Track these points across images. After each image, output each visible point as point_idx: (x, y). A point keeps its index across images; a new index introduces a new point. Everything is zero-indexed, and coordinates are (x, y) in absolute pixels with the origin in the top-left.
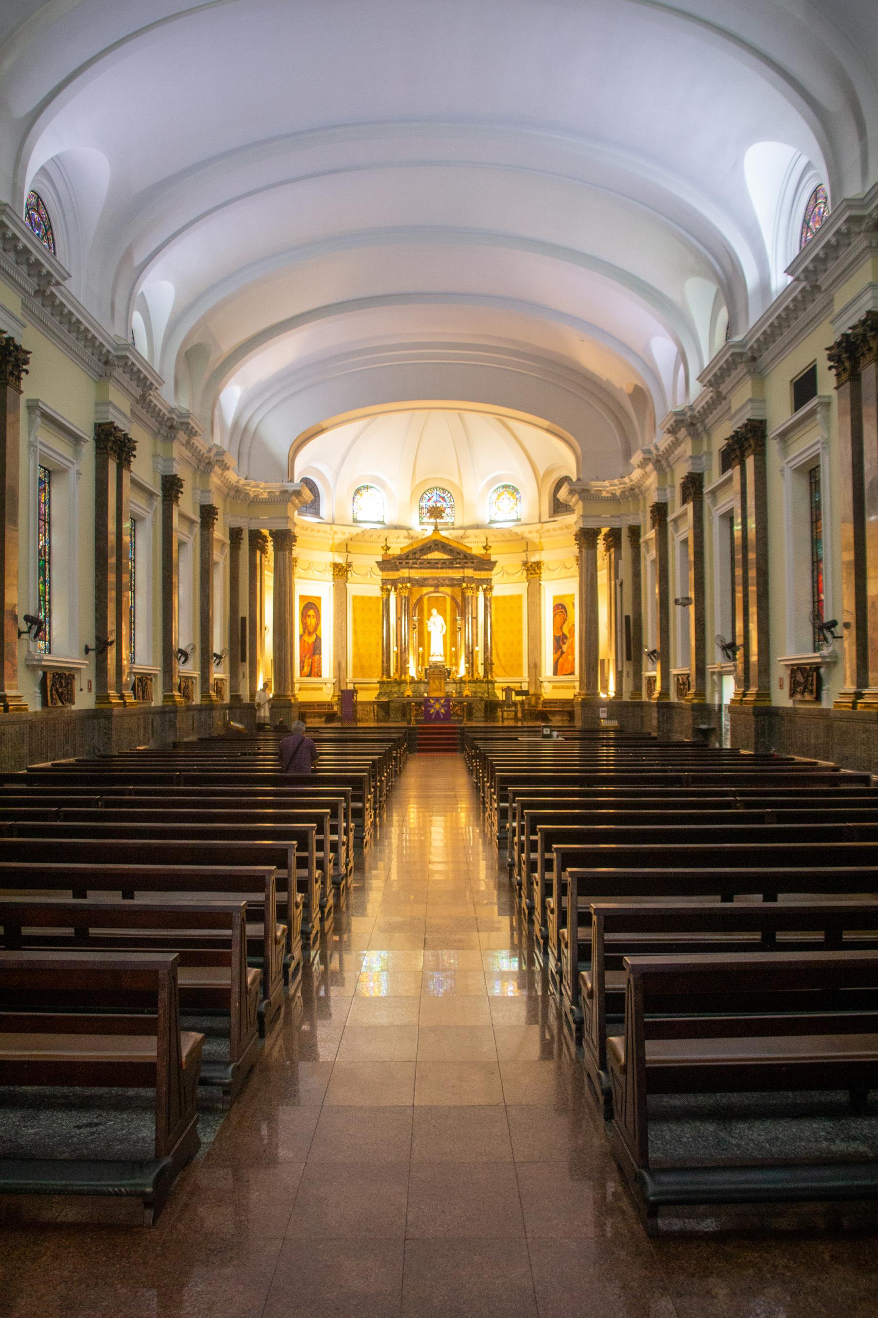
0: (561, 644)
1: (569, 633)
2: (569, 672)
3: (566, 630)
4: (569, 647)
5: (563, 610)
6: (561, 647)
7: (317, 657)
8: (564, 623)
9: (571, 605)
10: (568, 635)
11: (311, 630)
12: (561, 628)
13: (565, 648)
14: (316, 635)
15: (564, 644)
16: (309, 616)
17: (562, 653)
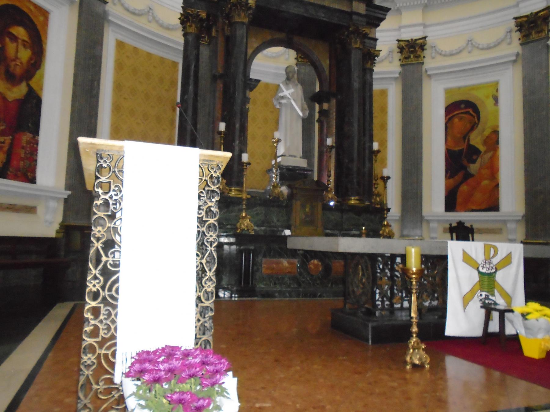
0: (465, 162)
1: (485, 142)
2: (483, 206)
3: (476, 140)
4: (481, 168)
5: (471, 111)
6: (465, 168)
7: (26, 137)
8: (472, 129)
9: (491, 101)
10: (482, 148)
11: (18, 71)
12: (465, 136)
13: (473, 168)
14: (28, 86)
15: (474, 162)
16: (14, 38)
17: (468, 176)
